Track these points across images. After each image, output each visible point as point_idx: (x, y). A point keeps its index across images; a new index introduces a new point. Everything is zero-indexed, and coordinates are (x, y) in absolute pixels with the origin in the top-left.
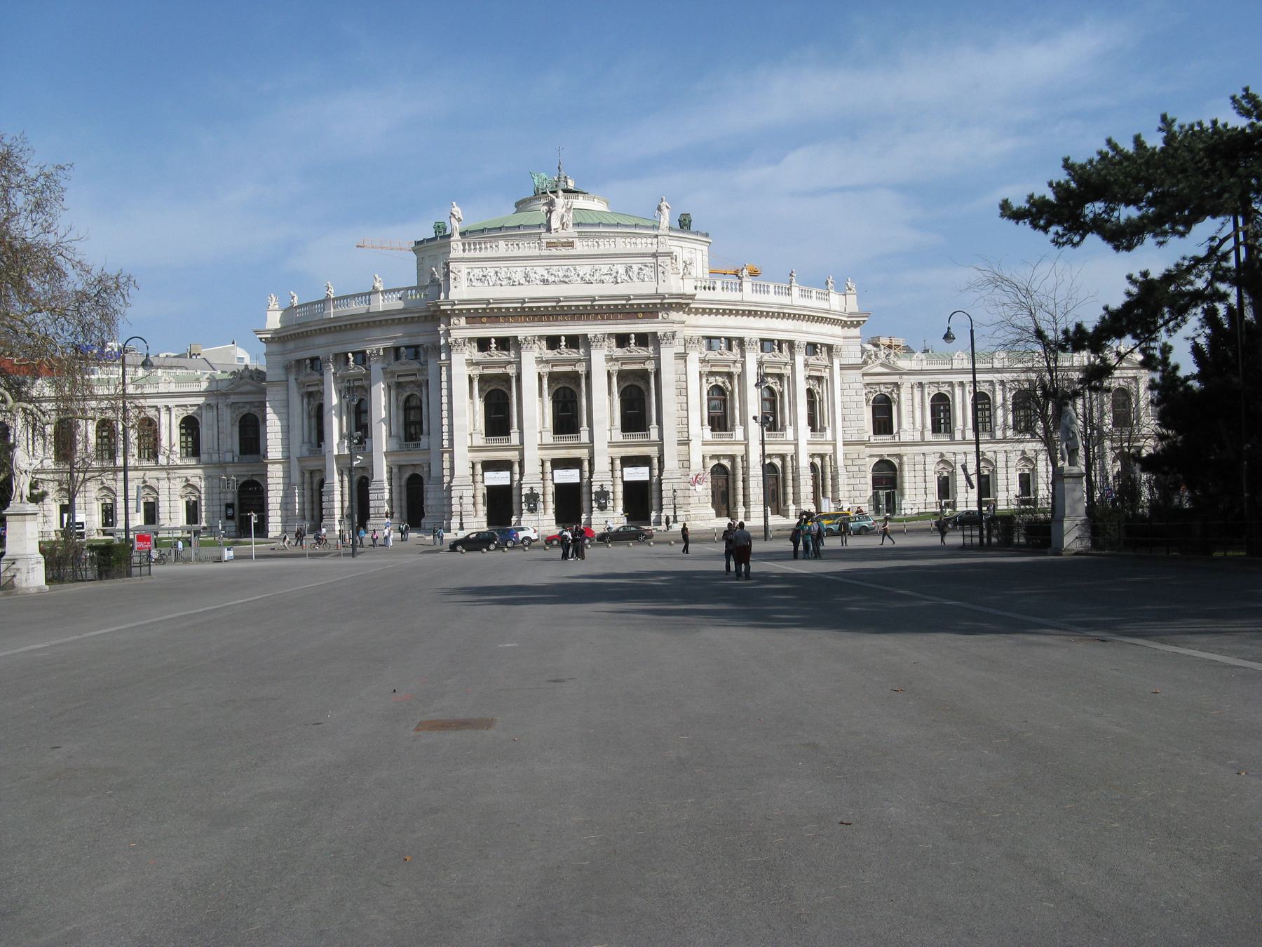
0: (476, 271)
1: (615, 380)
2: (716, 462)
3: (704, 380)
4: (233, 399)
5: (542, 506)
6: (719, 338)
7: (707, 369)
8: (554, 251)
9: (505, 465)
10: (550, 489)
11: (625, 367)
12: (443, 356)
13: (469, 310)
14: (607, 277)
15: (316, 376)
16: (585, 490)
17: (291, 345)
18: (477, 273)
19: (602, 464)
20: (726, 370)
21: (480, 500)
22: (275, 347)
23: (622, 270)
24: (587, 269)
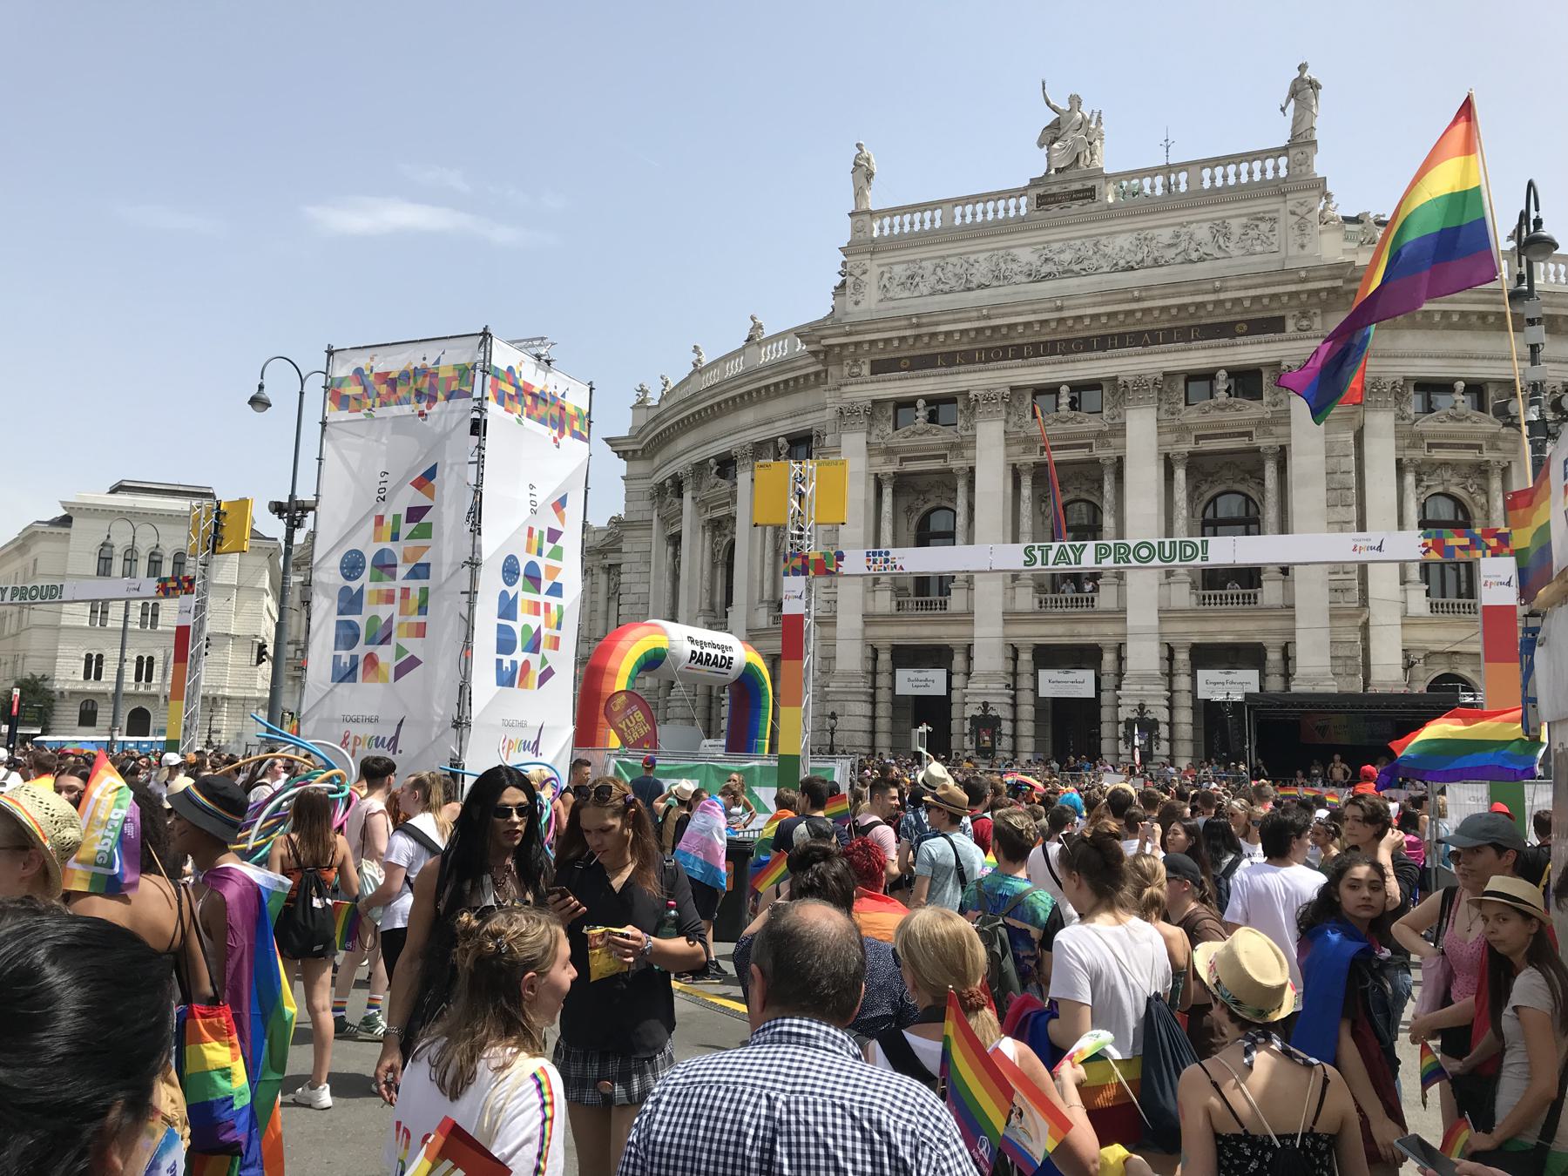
0: (898, 269)
1: (1180, 474)
2: (1441, 669)
3: (1410, 479)
4: (612, 559)
5: (1006, 743)
6: (1446, 386)
7: (1419, 454)
8: (1054, 208)
9: (936, 656)
10: (1027, 711)
11: (1207, 445)
12: (828, 440)
13: (872, 343)
14: (1171, 253)
15: (676, 500)
16: (1106, 714)
17: (657, 461)
18: (900, 271)
19: (1144, 657)
20: (1469, 456)
21: (883, 724)
22: (641, 467)
23: (1202, 233)
24: (1124, 241)
